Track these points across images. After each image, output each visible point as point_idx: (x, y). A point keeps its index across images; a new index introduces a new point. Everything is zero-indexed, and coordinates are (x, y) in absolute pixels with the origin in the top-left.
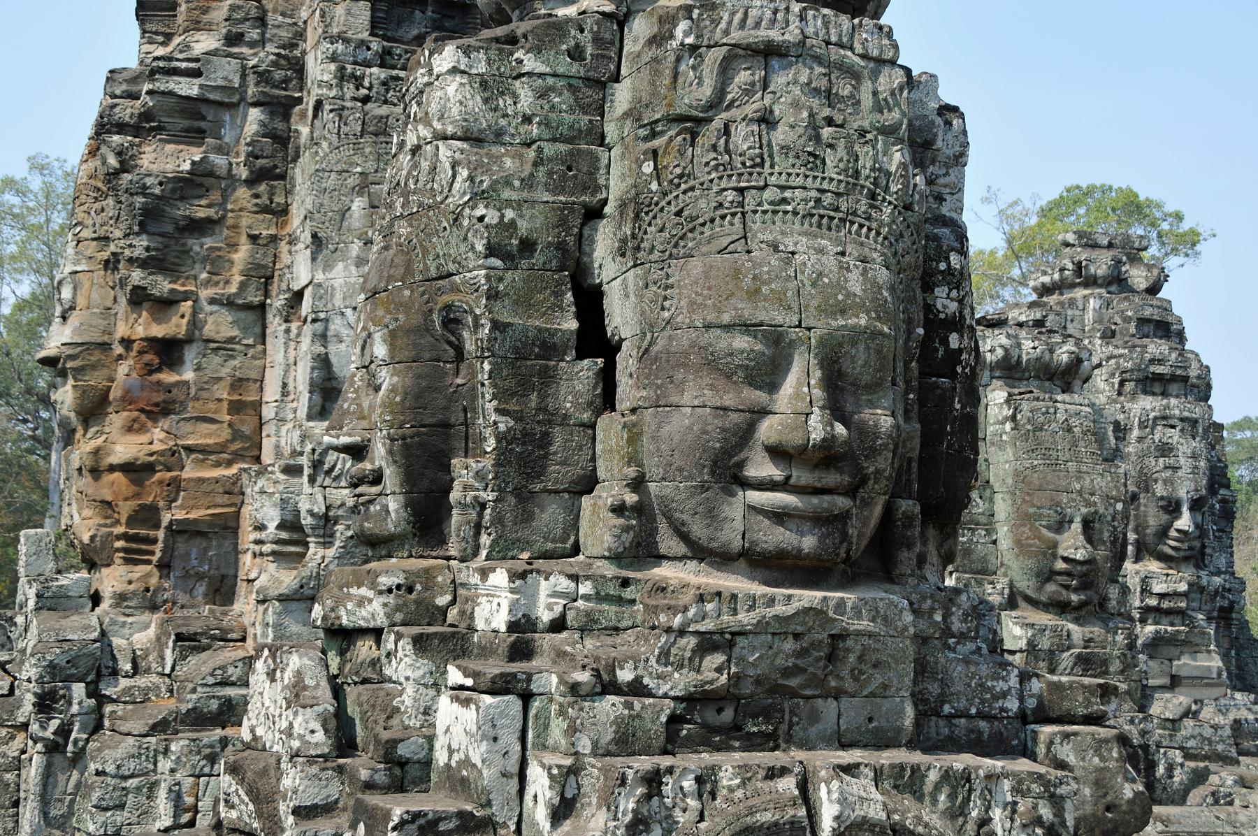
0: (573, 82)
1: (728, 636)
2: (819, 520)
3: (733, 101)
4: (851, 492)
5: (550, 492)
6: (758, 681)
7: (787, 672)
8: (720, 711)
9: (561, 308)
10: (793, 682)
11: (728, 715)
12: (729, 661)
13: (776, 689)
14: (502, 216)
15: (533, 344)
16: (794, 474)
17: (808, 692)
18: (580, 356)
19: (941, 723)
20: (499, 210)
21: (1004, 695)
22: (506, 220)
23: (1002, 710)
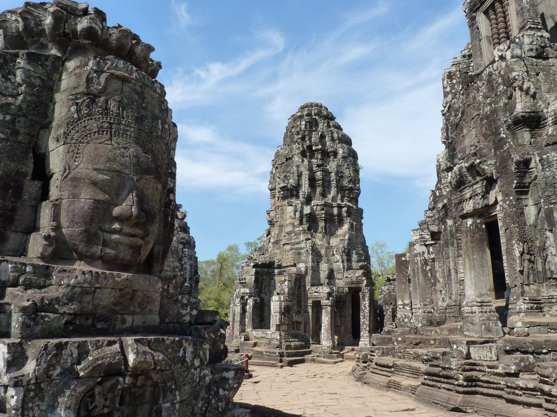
0: (42, 77)
1: (93, 289)
2: (131, 247)
3: (110, 93)
4: (143, 238)
5: (13, 231)
6: (104, 308)
7: (115, 304)
8: (87, 319)
9: (27, 159)
10: (117, 308)
11: (90, 321)
12: (93, 299)
13: (110, 310)
14: (5, 118)
15: (13, 170)
16: (124, 228)
17: (123, 312)
18: (34, 178)
19: (165, 325)
20: (4, 115)
21: (185, 315)
22: (6, 120)
23: (184, 320)
